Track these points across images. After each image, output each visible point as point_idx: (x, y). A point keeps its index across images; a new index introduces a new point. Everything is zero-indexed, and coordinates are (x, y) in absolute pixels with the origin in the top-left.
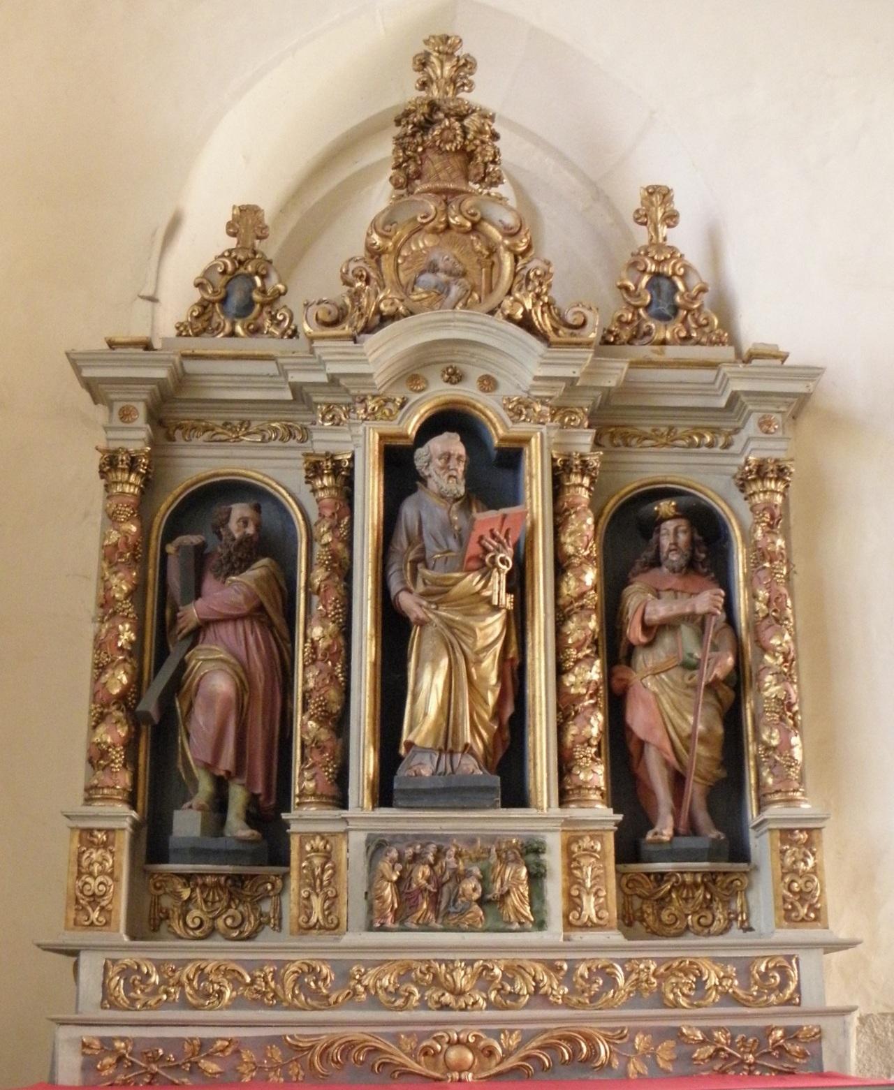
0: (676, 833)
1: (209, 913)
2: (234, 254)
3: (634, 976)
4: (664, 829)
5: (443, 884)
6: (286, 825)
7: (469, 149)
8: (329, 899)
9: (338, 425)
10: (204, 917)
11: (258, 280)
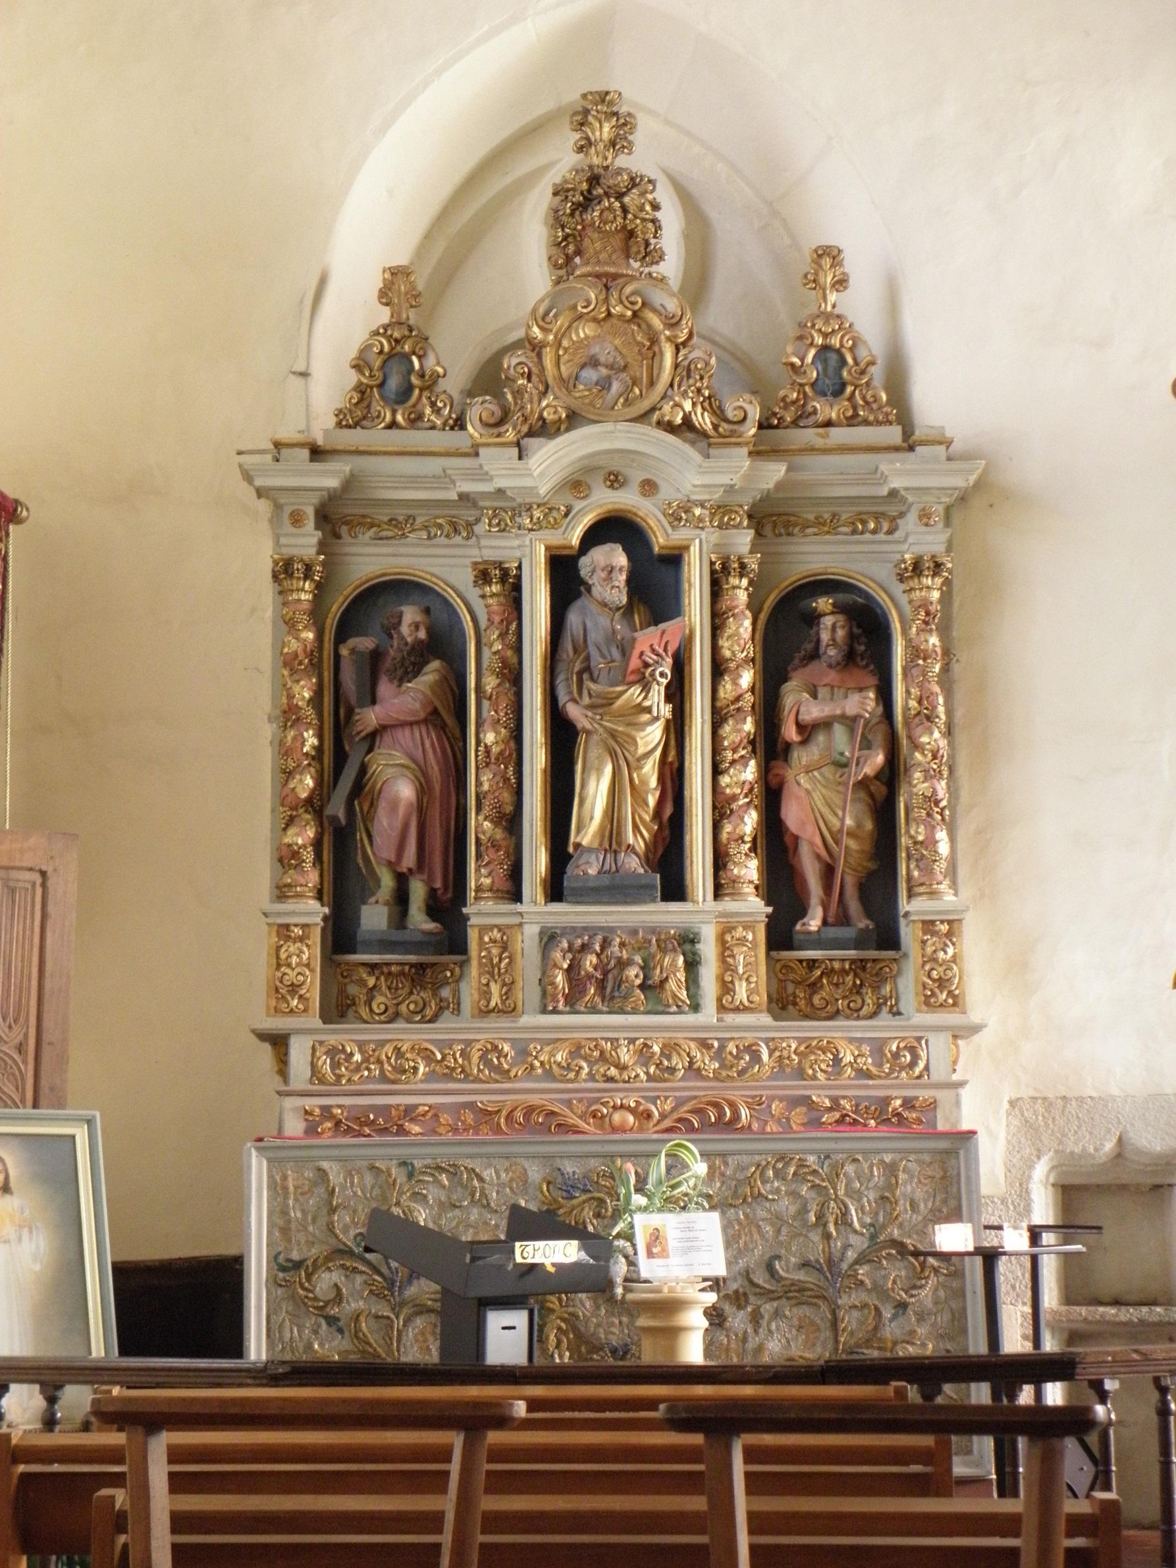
0: (825, 922)
3: (777, 1054)
4: (814, 922)
6: (466, 918)
7: (629, 228)
9: (504, 530)
11: (415, 359)
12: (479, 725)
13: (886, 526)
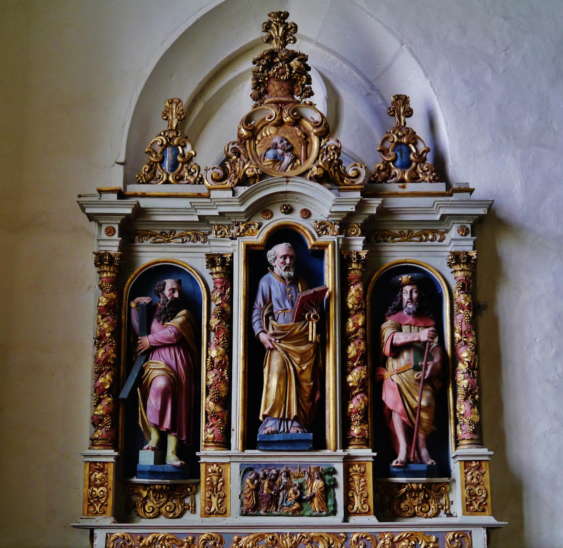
1: (157, 504)
2: (166, 134)
5: (280, 491)
6: (199, 458)
8: (221, 498)
9: (224, 237)
10: (155, 507)
11: (180, 148)
12: (208, 347)
13: (438, 237)
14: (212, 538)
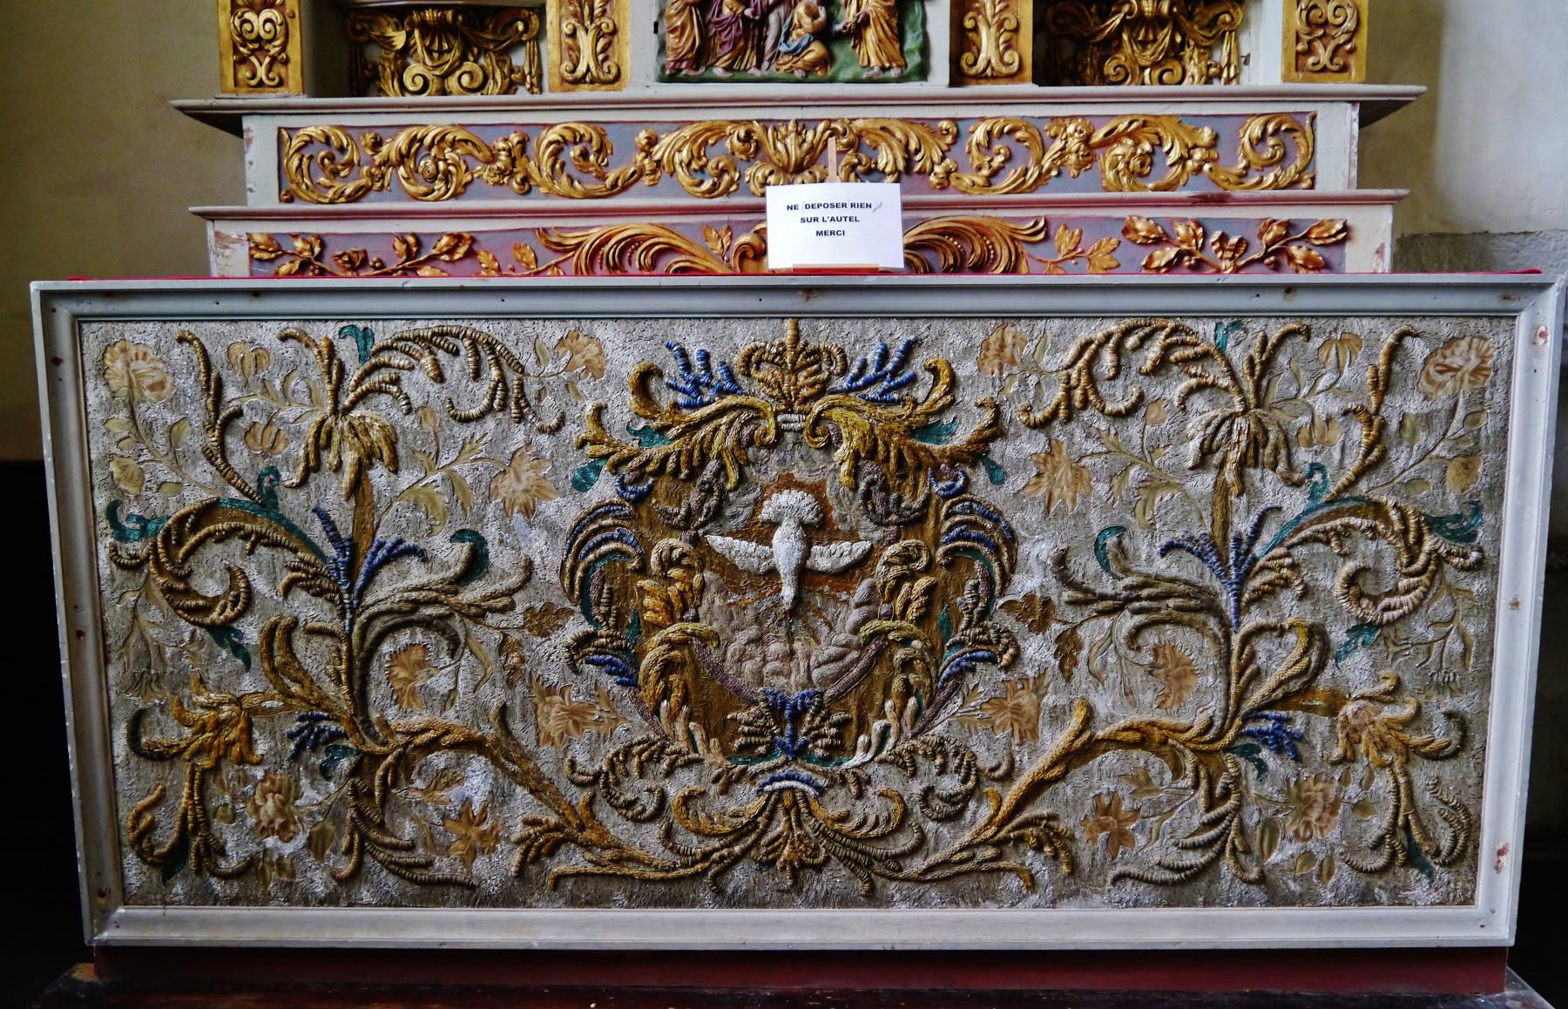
1: (435, 68)
8: (603, 36)
10: (429, 76)
14: (578, 139)
